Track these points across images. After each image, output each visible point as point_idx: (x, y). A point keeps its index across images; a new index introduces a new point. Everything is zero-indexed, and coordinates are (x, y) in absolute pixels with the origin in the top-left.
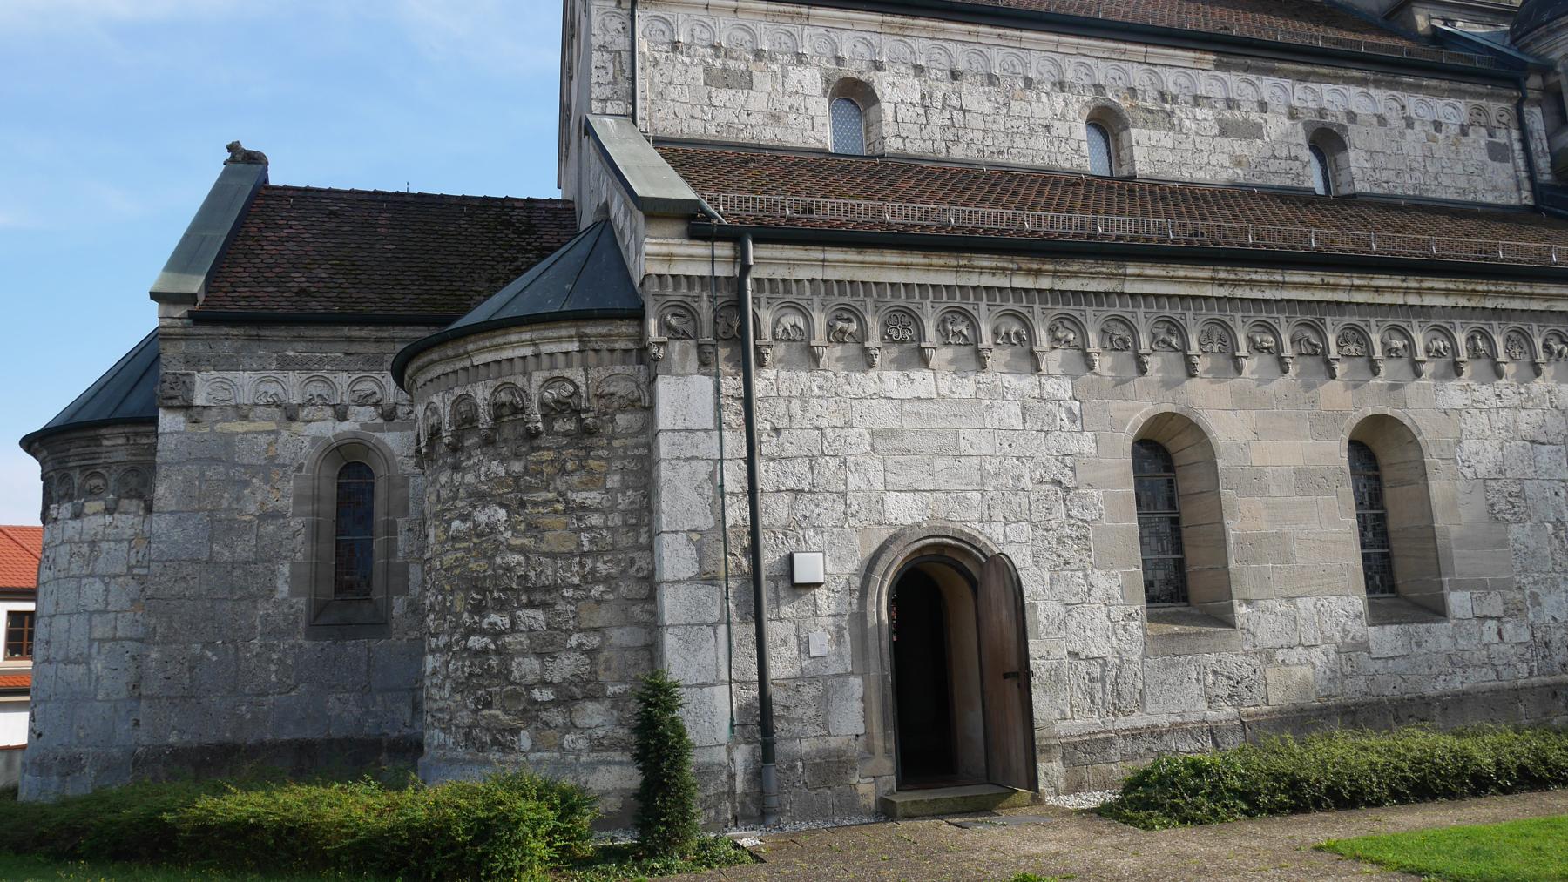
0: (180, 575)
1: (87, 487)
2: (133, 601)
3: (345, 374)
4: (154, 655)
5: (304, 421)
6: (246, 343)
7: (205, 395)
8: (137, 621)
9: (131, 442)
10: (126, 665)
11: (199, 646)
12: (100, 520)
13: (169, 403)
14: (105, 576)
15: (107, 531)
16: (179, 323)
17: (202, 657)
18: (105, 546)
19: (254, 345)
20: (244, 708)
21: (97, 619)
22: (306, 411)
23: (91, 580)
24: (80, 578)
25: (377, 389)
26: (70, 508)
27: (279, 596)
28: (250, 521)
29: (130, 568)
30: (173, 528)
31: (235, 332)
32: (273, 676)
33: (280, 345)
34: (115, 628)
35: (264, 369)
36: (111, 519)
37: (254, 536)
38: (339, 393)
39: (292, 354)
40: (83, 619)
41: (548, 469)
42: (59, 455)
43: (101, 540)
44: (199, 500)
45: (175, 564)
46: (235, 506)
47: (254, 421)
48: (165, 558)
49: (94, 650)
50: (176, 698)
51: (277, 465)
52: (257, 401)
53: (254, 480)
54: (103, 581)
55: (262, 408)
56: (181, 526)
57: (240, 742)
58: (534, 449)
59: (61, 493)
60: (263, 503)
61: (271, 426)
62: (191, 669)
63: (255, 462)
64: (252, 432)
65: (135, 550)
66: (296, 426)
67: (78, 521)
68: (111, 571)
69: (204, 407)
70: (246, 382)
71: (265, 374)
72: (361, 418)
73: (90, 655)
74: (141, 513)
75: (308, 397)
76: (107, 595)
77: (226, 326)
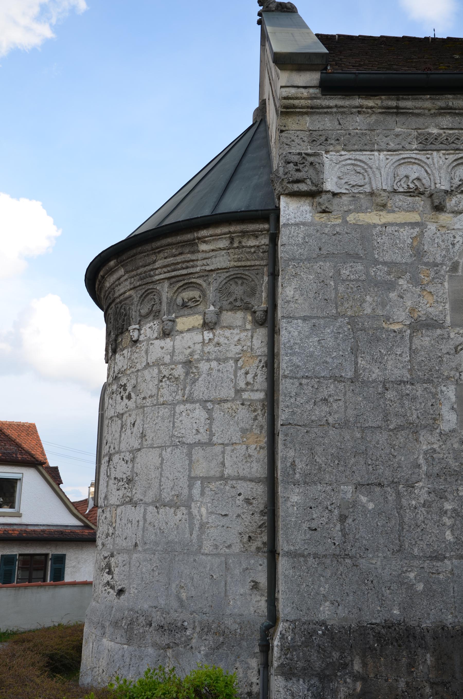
0: (320, 396)
1: (179, 301)
2: (244, 431)
4: (295, 498)
5: (453, 212)
6: (381, 117)
7: (335, 179)
8: (250, 456)
9: (236, 245)
10: (239, 511)
11: (350, 488)
12: (197, 337)
13: (296, 187)
14: (206, 401)
15: (206, 349)
16: (305, 93)
17: (355, 503)
18: (204, 366)
19: (391, 120)
20: (412, 575)
21: (198, 453)
22: (454, 200)
23: (188, 406)
24: (174, 405)
26: (156, 327)
27: (445, 427)
28: (400, 332)
29: (238, 392)
30: (307, 337)
31: (370, 103)
32: (448, 533)
33: (421, 120)
34: (223, 464)
35: (404, 149)
36: (211, 336)
37: (407, 349)
39: (435, 131)
40: (180, 453)
42: (142, 270)
43: (198, 361)
44: (336, 304)
45: (314, 382)
46: (379, 312)
47: (394, 212)
48: (301, 374)
49: (196, 491)
50: (325, 556)
51: (426, 264)
52: (396, 187)
53: (401, 282)
54: (205, 408)
55: (401, 197)
56: (317, 335)
57: (413, 623)
59: (144, 312)
60: (413, 310)
61: (415, 217)
62: (343, 518)
63: (399, 259)
64: (392, 224)
65: (243, 371)
66: (444, 218)
67: (168, 340)
68: (214, 395)
69: (335, 195)
70: (382, 164)
71: (406, 154)
73: (190, 497)
74: (249, 326)
76: (211, 424)
77: (360, 96)
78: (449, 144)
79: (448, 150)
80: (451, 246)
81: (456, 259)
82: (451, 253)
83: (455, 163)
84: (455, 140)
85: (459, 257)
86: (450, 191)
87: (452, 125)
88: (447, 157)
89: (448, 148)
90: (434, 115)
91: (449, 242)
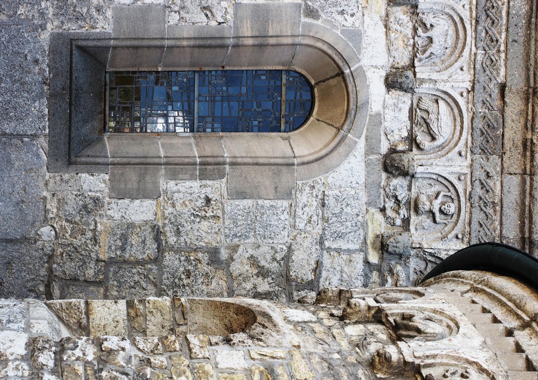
3: (469, 85)
5: (387, 16)
25: (440, 141)
38: (434, 76)
72: (389, 114)
75: (429, 20)
78: (485, 11)
79: (477, 8)
80: (340, 9)
81: (323, 15)
82: (330, 9)
83: (457, 19)
84: (491, 19)
85: (325, 20)
86: (418, 12)
87: (515, 15)
88: (467, 7)
89: (480, 8)
91: (346, 8)
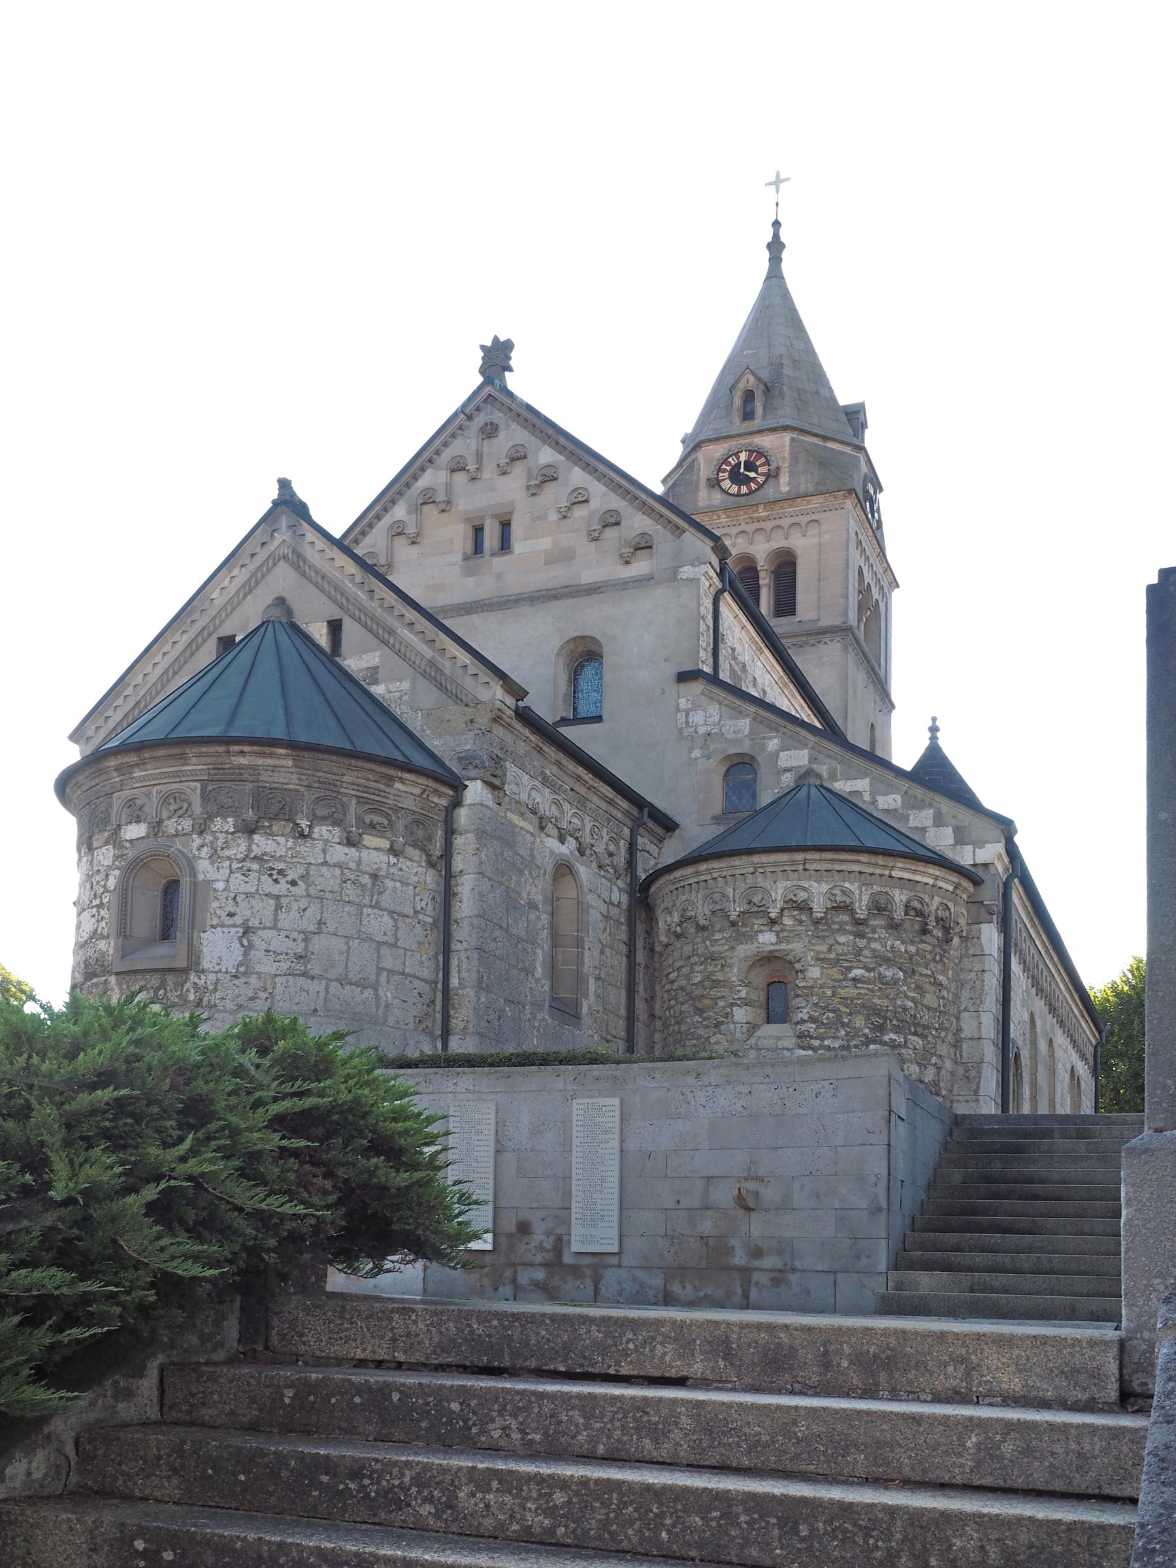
1: (367, 820)
2: (420, 943)
9: (424, 796)
10: (415, 1001)
15: (392, 870)
21: (385, 951)
23: (376, 911)
41: (928, 956)
43: (384, 877)
54: (392, 917)
58: (922, 942)
68: (398, 909)
73: (378, 982)
74: (424, 864)
76: (396, 931)
90: (551, 762)
